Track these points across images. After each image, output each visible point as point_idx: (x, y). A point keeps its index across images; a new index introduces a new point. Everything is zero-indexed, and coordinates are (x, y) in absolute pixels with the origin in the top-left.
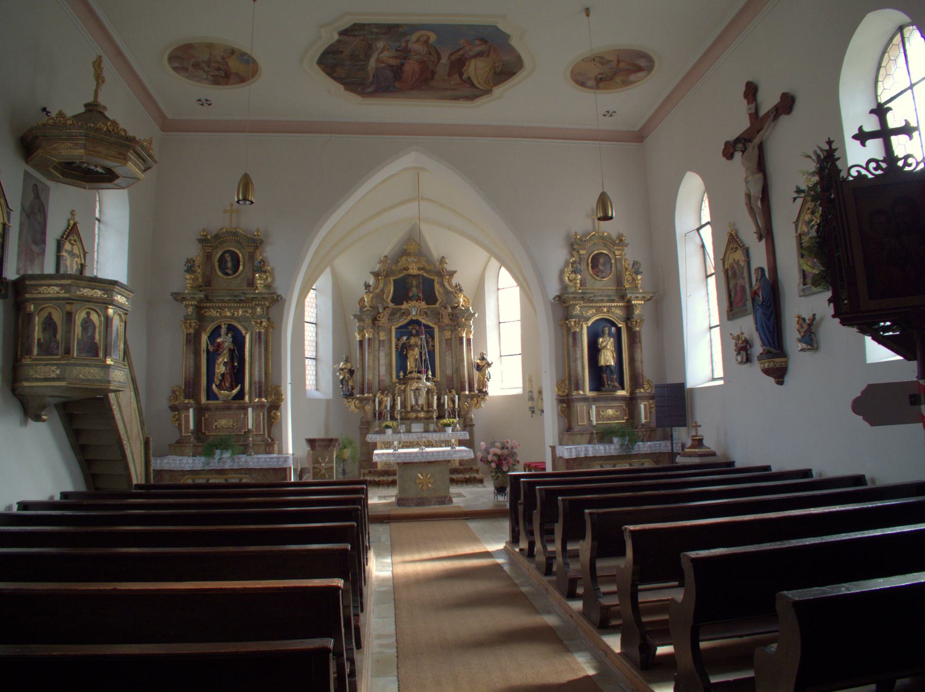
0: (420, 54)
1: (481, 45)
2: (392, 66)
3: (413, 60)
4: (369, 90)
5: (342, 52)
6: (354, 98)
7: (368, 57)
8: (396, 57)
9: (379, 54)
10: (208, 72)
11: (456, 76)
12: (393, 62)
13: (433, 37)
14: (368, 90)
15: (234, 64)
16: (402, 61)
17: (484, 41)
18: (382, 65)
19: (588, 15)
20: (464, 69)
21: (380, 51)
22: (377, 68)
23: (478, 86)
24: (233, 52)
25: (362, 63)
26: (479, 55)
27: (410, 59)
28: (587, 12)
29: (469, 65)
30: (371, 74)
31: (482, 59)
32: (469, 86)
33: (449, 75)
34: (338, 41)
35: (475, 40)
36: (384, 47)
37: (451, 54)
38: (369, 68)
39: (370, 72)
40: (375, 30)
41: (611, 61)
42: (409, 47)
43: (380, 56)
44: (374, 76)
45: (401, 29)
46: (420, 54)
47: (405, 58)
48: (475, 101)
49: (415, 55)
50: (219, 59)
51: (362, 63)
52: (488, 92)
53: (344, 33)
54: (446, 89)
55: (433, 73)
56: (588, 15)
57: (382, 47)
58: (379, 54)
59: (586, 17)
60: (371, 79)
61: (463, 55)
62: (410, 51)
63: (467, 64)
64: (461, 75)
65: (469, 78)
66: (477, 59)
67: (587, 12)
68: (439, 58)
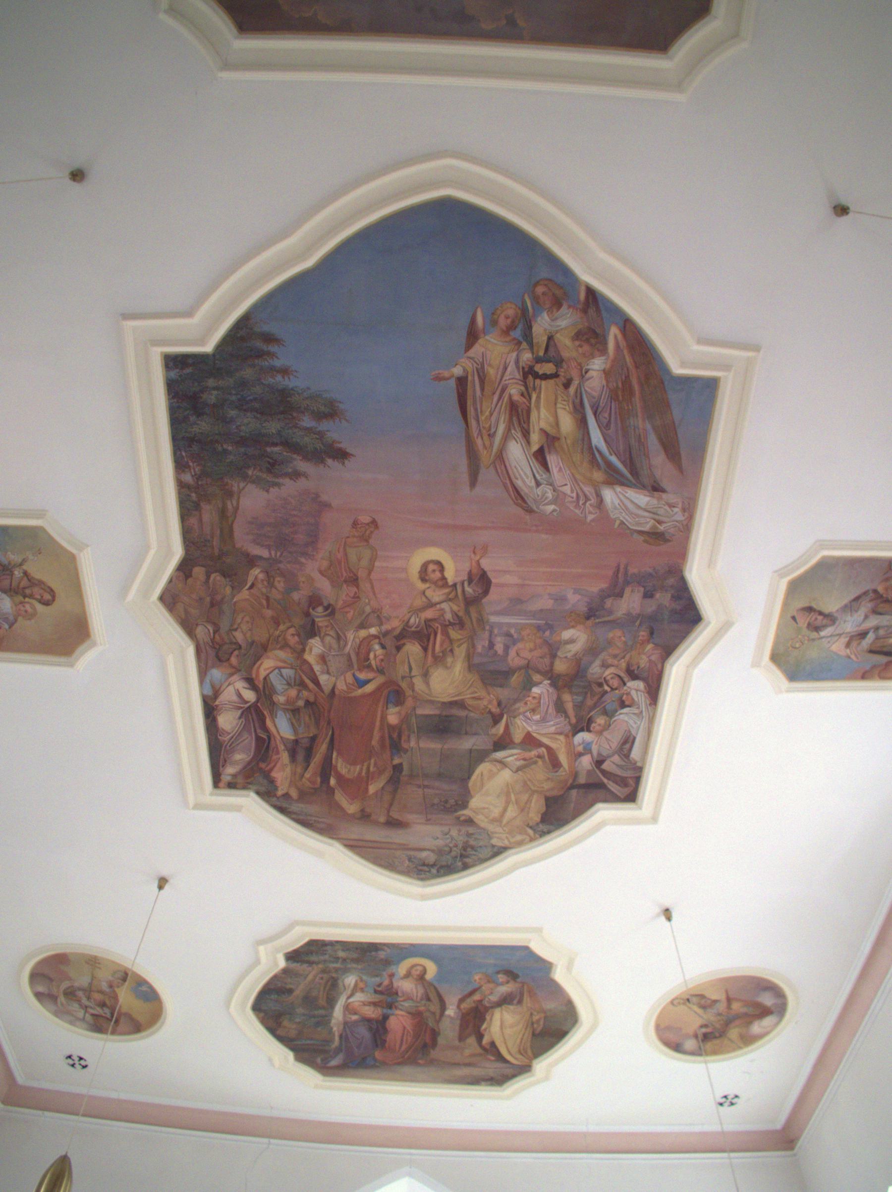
0: (412, 999)
1: (508, 982)
2: (369, 1020)
3: (401, 1010)
4: (333, 1063)
5: (290, 991)
6: (308, 1075)
7: (331, 1002)
8: (375, 1004)
9: (349, 998)
10: (86, 1007)
11: (472, 1040)
12: (370, 1012)
13: (432, 970)
14: (333, 1063)
15: (125, 998)
16: (385, 1011)
17: (512, 975)
18: (355, 1017)
19: (669, 919)
20: (484, 1027)
21: (349, 992)
22: (346, 1023)
23: (508, 1057)
24: (125, 975)
25: (322, 1012)
26: (506, 1000)
27: (396, 1008)
28: (667, 914)
29: (491, 1019)
30: (337, 1034)
31: (511, 1007)
32: (493, 1058)
33: (461, 1038)
34: (285, 971)
35: (498, 972)
36: (356, 985)
37: (461, 1001)
38: (333, 1021)
39: (335, 1029)
40: (341, 954)
41: (715, 1002)
42: (395, 984)
43: (351, 1000)
44: (341, 1036)
45: (382, 955)
46: (412, 999)
47: (390, 1006)
48: (505, 1086)
49: (404, 1001)
50: (104, 986)
51: (322, 1012)
52: (525, 1069)
53: (293, 956)
54: (456, 1065)
55: (435, 1034)
56: (669, 919)
57: (353, 982)
58: (349, 998)
59: (667, 923)
60: (336, 1042)
61: (480, 1001)
62: (397, 993)
63: (488, 1017)
64: (480, 1037)
65: (493, 1044)
66: (503, 1007)
67: (667, 914)
68: (443, 1007)
